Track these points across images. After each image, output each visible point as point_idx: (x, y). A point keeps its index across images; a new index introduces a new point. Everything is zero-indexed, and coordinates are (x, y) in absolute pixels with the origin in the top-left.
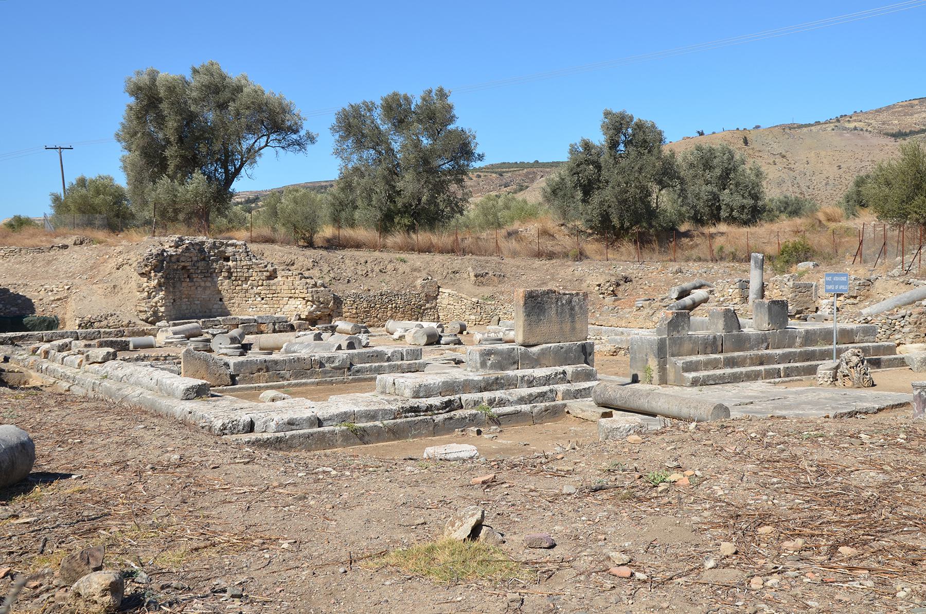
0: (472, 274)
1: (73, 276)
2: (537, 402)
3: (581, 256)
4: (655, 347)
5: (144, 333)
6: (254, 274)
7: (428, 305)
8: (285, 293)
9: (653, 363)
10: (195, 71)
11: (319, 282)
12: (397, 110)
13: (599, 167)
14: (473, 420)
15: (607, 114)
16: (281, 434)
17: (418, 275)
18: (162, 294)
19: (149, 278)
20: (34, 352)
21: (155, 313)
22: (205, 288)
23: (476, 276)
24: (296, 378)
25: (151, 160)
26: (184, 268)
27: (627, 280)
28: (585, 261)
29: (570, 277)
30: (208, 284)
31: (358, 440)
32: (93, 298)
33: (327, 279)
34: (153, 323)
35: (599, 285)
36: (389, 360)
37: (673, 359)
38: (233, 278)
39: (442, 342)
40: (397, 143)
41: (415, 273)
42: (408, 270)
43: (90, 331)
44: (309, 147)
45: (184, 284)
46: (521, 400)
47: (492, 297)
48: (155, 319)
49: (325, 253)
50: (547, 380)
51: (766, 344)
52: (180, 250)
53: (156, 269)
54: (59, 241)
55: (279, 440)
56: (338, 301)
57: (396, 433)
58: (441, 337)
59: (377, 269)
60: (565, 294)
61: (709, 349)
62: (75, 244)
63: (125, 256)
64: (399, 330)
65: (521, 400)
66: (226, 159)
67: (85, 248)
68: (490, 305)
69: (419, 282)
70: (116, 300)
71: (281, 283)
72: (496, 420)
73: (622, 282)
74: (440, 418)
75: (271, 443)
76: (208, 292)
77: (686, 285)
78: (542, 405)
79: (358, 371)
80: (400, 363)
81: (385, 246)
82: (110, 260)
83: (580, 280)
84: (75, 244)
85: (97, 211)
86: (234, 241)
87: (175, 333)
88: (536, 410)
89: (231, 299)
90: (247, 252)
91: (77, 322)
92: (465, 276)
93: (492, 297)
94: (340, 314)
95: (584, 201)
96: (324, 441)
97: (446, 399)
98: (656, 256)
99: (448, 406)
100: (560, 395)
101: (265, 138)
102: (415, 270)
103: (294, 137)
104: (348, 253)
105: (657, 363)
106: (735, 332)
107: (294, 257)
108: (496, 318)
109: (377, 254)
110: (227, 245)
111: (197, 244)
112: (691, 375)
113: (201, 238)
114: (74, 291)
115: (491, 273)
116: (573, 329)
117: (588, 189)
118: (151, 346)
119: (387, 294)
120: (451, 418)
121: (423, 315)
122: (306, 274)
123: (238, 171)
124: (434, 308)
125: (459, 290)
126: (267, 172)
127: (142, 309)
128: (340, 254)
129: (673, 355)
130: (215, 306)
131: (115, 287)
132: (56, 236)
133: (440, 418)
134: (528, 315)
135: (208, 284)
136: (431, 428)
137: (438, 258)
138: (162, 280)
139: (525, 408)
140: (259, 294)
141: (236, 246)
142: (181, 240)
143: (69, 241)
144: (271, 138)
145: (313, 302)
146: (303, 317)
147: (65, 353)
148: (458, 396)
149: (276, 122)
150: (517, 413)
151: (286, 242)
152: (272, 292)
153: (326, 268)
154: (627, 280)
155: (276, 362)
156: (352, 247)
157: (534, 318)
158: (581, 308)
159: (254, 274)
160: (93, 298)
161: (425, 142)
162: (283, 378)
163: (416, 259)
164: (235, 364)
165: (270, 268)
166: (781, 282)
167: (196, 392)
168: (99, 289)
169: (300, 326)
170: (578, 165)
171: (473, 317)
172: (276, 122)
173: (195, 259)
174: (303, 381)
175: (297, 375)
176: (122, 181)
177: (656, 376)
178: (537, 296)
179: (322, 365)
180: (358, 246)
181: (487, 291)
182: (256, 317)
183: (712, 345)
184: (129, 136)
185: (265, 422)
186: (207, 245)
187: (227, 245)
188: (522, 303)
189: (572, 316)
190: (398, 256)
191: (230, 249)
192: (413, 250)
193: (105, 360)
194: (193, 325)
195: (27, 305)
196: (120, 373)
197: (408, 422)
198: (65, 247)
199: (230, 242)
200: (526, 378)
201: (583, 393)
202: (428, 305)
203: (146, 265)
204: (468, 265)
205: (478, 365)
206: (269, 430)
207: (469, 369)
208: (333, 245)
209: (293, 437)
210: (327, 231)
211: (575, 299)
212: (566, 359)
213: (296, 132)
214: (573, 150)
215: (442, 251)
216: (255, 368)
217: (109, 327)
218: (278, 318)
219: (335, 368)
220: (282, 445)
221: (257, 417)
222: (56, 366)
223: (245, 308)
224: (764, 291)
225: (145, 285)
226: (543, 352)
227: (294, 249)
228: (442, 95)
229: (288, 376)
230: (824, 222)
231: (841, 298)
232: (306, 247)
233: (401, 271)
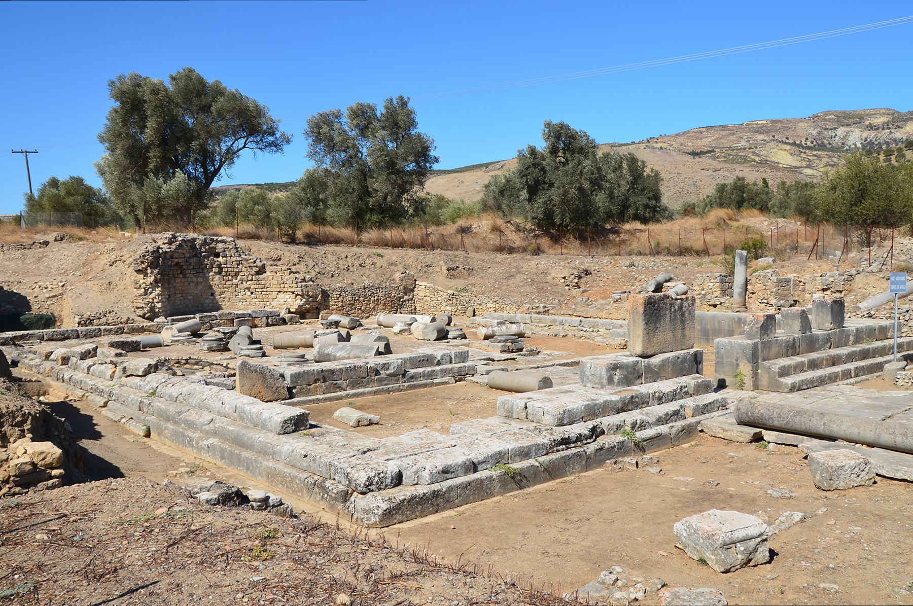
0: (444, 268)
1: (66, 273)
2: (672, 421)
3: (538, 251)
4: (749, 352)
5: (142, 330)
6: (244, 269)
7: (406, 297)
8: (274, 288)
9: (745, 368)
10: (173, 79)
11: (308, 277)
12: (364, 118)
13: (543, 170)
14: (621, 450)
15: (548, 125)
16: (436, 487)
17: (395, 269)
18: (158, 290)
19: (146, 275)
20: (48, 356)
22: (197, 284)
23: (448, 270)
24: (353, 387)
25: (134, 161)
26: (177, 264)
27: (587, 273)
28: (542, 255)
29: (535, 271)
30: (200, 280)
31: (514, 485)
32: (90, 295)
33: (313, 274)
34: (151, 319)
35: (564, 278)
36: (439, 363)
37: (767, 363)
38: (224, 274)
39: (449, 336)
40: (366, 148)
41: (392, 267)
42: (385, 264)
43: (89, 327)
44: (285, 147)
45: (178, 280)
46: (660, 421)
47: (465, 290)
48: (152, 315)
49: (307, 248)
50: (674, 396)
52: (173, 247)
53: (153, 265)
54: (40, 238)
55: (436, 494)
56: (325, 295)
57: (552, 472)
58: (448, 331)
59: (357, 263)
60: (677, 299)
62: (56, 240)
63: (118, 253)
64: (399, 324)
65: (660, 421)
66: (206, 157)
67: (64, 244)
68: (464, 297)
69: (398, 276)
70: (112, 296)
71: (271, 278)
72: (640, 447)
73: (583, 275)
74: (591, 448)
75: (428, 499)
76: (200, 287)
77: (660, 278)
78: (679, 424)
79: (412, 377)
80: (450, 366)
81: (360, 241)
82: (102, 257)
83: (545, 273)
84: (56, 240)
85: (70, 209)
86: (224, 238)
87: (180, 331)
88: (674, 431)
89: (221, 293)
90: (237, 248)
91: (77, 319)
92: (438, 269)
93: (465, 290)
94: (327, 307)
95: (530, 200)
96: (480, 490)
97: (590, 424)
98: (599, 251)
99: (596, 433)
100: (689, 412)
101: (243, 140)
102: (392, 264)
103: (271, 138)
104: (330, 248)
105: (750, 368)
106: (808, 334)
107: (281, 253)
108: (471, 309)
109: (355, 249)
110: (217, 242)
111: (189, 241)
112: (789, 380)
113: (191, 235)
114: (69, 288)
115: (461, 267)
116: (684, 336)
117: (533, 191)
118: (159, 345)
119: (370, 288)
120: (601, 449)
121: (401, 306)
122: (294, 269)
123: (217, 171)
124: (411, 300)
125: (433, 282)
126: (247, 170)
127: (139, 305)
128: (321, 250)
129: (764, 360)
130: (207, 301)
131: (110, 283)
132: (36, 233)
133: (591, 448)
134: (647, 324)
135: (200, 280)
136: (584, 463)
137: (412, 253)
138: (159, 277)
139: (663, 429)
140: (249, 289)
141: (225, 242)
142: (174, 237)
143: (50, 237)
144: (250, 140)
145: (302, 296)
146: (293, 310)
147: (89, 361)
148: (598, 420)
149: (251, 124)
150: (659, 436)
151: (270, 238)
152: (261, 286)
153: (311, 264)
154: (587, 273)
155: (332, 372)
156: (330, 243)
157: (652, 326)
158: (690, 313)
159: (244, 269)
160: (90, 295)
161: (390, 145)
162: (340, 388)
163: (391, 254)
164: (292, 376)
165: (258, 263)
166: (765, 277)
167: (295, 424)
168: (94, 286)
169: (291, 319)
170: (527, 169)
171: (449, 308)
172: (251, 124)
173: (188, 255)
174: (361, 390)
175: (353, 385)
176: (96, 182)
177: (748, 381)
178: (655, 302)
179: (377, 373)
180: (337, 241)
181: (459, 283)
182: (250, 312)
183: (792, 349)
184: (112, 137)
185: (416, 472)
186: (198, 242)
187: (217, 242)
188: (641, 310)
189: (683, 322)
190: (374, 251)
191: (220, 245)
192: (386, 245)
193: (146, 373)
194: (195, 320)
195: (22, 303)
196: (174, 391)
197: (563, 457)
198: (46, 243)
199: (220, 238)
200: (657, 395)
202: (406, 297)
203: (142, 262)
204: (439, 259)
205: (605, 381)
206: (422, 481)
207: (589, 385)
208: (312, 240)
209: (450, 489)
210: (306, 228)
211: (685, 304)
212: (682, 369)
213: (273, 134)
214: (521, 156)
215: (414, 246)
216: (312, 378)
217: (109, 325)
218: (271, 313)
219: (390, 375)
220: (440, 500)
221: (405, 465)
222: (79, 375)
223: (236, 301)
224: (747, 285)
225: (142, 281)
226: (664, 363)
227: (279, 245)
228: (403, 103)
229: (344, 386)
230: (728, 222)
231: (828, 292)
232: (289, 243)
233: (378, 265)
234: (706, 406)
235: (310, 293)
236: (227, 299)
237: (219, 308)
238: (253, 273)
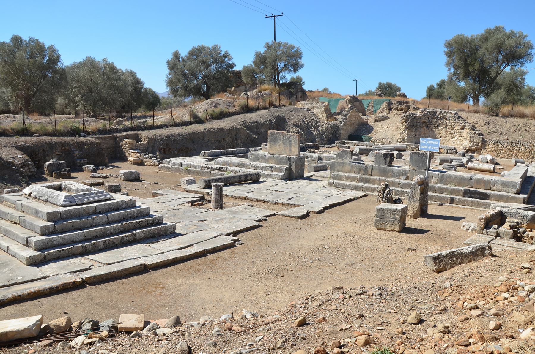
21: (403, 139)
51: (406, 177)
53: (406, 121)
61: (362, 172)
110: (447, 113)
157: (272, 143)
187: (447, 113)
191: (448, 115)
234: (268, 175)
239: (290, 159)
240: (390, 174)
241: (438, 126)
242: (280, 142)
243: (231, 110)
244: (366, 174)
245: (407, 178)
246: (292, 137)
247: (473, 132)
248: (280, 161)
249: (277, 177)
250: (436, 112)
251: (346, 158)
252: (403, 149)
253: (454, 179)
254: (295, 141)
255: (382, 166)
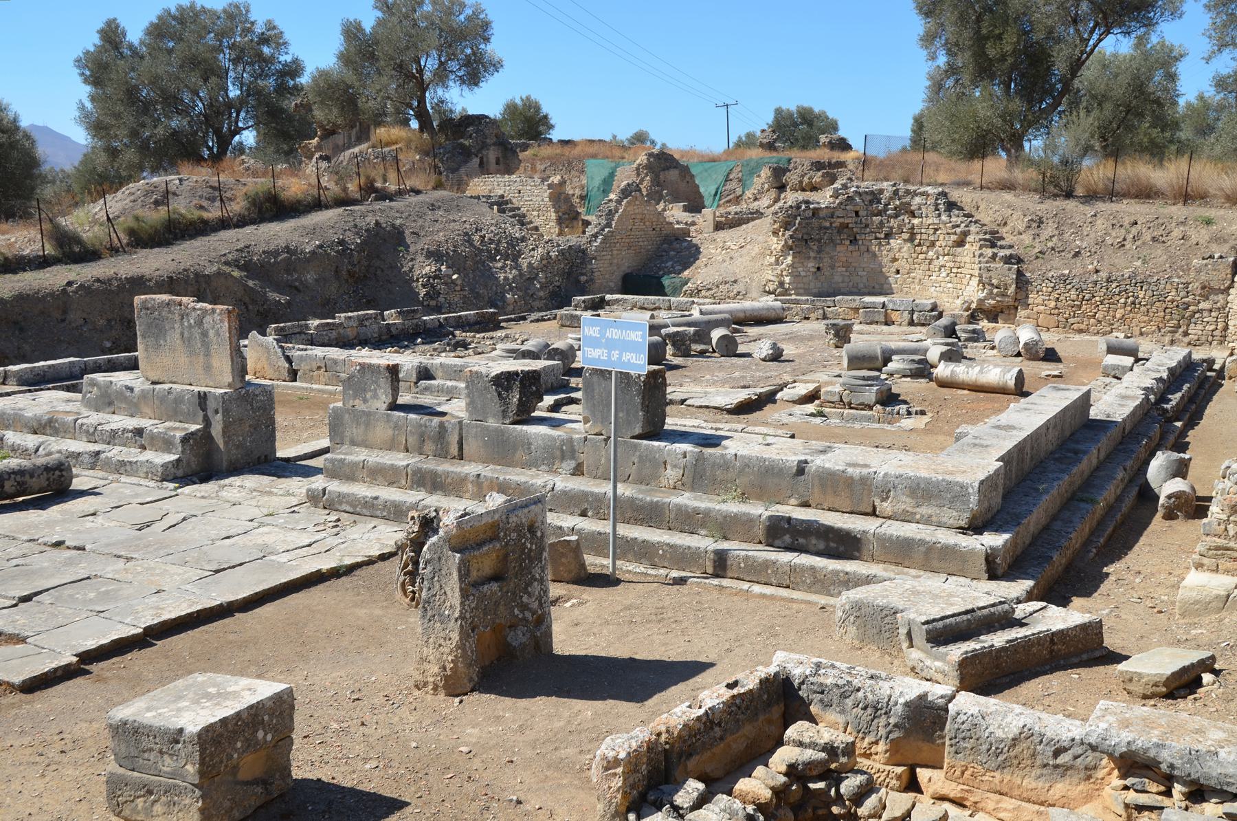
21: (781, 284)
38: (917, 242)
45: (839, 248)
51: (573, 464)
53: (786, 225)
61: (429, 447)
110: (915, 194)
155: (335, 362)
157: (151, 341)
187: (915, 194)
191: (918, 200)
201: (128, 468)
216: (315, 366)
234: (123, 463)
235: (995, 282)
236: (917, 281)
237: (882, 289)
238: (950, 243)
239: (202, 398)
240: (520, 454)
241: (888, 236)
242: (174, 337)
243: (214, 213)
244: (442, 454)
245: (578, 471)
246: (208, 319)
247: (989, 252)
248: (171, 408)
249: (149, 471)
250: (881, 191)
251: (375, 396)
252: (773, 315)
253: (741, 472)
254: (218, 334)
255: (492, 423)
